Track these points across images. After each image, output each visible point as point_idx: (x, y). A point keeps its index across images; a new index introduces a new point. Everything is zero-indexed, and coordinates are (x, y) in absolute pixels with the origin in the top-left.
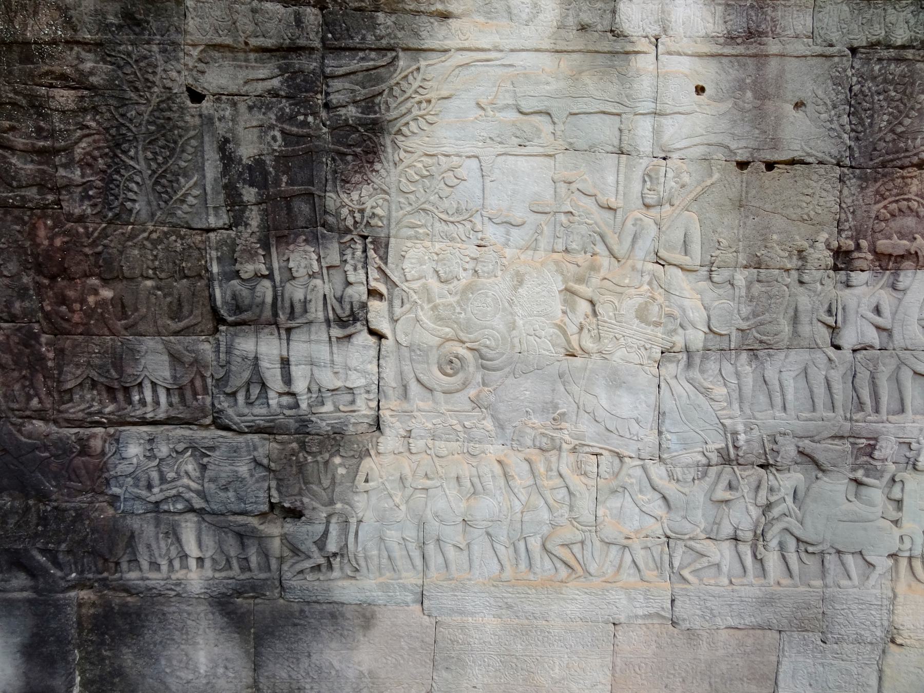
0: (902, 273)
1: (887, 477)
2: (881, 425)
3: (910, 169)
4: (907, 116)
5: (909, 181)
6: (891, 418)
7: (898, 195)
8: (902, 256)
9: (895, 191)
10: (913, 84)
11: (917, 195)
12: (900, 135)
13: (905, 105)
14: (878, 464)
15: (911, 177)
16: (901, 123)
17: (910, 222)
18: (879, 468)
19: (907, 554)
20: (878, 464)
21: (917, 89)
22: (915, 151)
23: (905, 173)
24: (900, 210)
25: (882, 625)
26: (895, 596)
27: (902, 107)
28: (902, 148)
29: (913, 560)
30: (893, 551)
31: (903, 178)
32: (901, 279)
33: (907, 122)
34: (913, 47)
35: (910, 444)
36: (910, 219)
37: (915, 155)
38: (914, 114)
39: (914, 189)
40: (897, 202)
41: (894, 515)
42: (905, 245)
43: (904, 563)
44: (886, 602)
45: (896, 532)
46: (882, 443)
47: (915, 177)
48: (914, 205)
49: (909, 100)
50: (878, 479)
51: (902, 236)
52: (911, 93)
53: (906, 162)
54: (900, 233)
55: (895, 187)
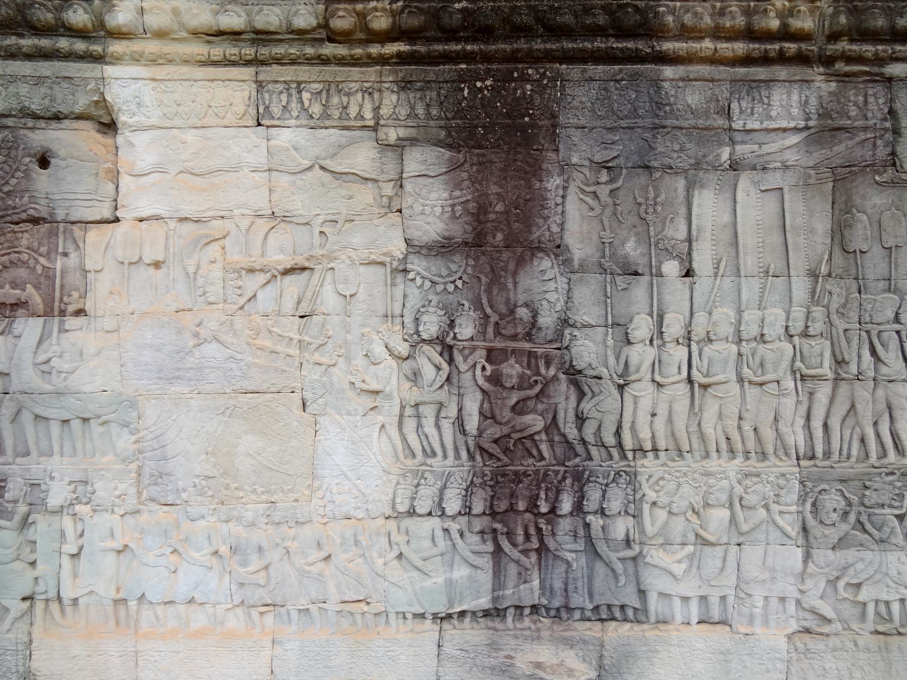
0: (17, 320)
1: (17, 518)
2: (7, 467)
3: (21, 225)
4: (13, 177)
5: (20, 235)
6: (18, 460)
7: (9, 248)
8: (16, 304)
9: (6, 245)
10: (17, 148)
11: (28, 248)
12: (8, 193)
13: (11, 166)
14: (10, 506)
15: (22, 232)
16: (7, 183)
17: (22, 273)
18: (10, 509)
19: (43, 597)
20: (10, 506)
21: (20, 152)
22: (23, 208)
23: (16, 228)
24: (11, 262)
25: (17, 671)
26: (31, 641)
27: (7, 168)
28: (10, 205)
29: (50, 603)
30: (27, 593)
31: (15, 232)
32: (15, 326)
33: (13, 181)
34: (14, 116)
35: (39, 485)
36: (22, 270)
37: (25, 211)
38: (20, 174)
39: (24, 242)
40: (9, 254)
41: (32, 558)
42: (15, 294)
43: (39, 606)
44: (20, 647)
45: (30, 574)
46: (10, 485)
47: (26, 231)
48: (25, 257)
49: (15, 162)
50: (10, 520)
51: (15, 285)
52: (16, 156)
53: (15, 218)
54: (14, 282)
55: (7, 241)
